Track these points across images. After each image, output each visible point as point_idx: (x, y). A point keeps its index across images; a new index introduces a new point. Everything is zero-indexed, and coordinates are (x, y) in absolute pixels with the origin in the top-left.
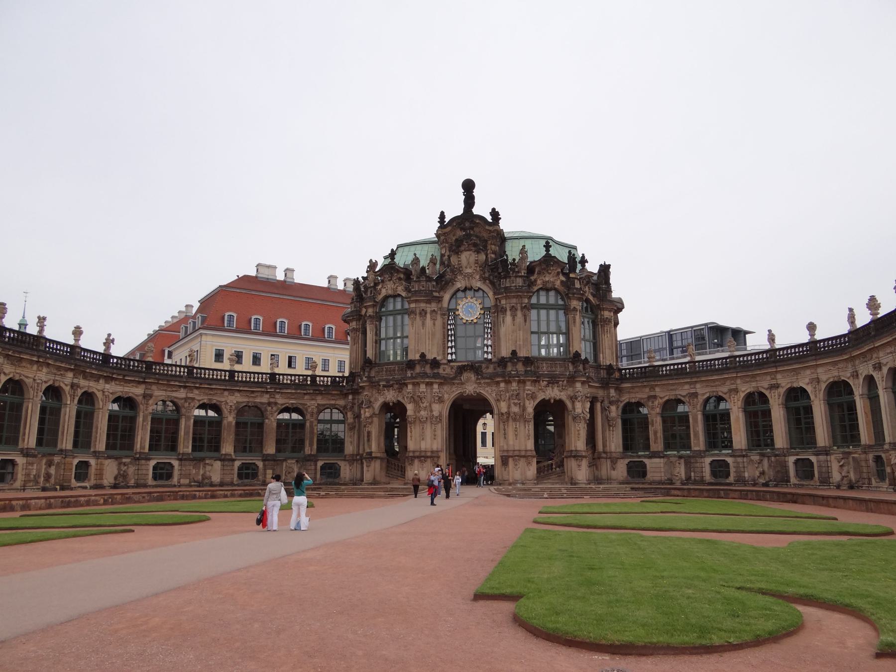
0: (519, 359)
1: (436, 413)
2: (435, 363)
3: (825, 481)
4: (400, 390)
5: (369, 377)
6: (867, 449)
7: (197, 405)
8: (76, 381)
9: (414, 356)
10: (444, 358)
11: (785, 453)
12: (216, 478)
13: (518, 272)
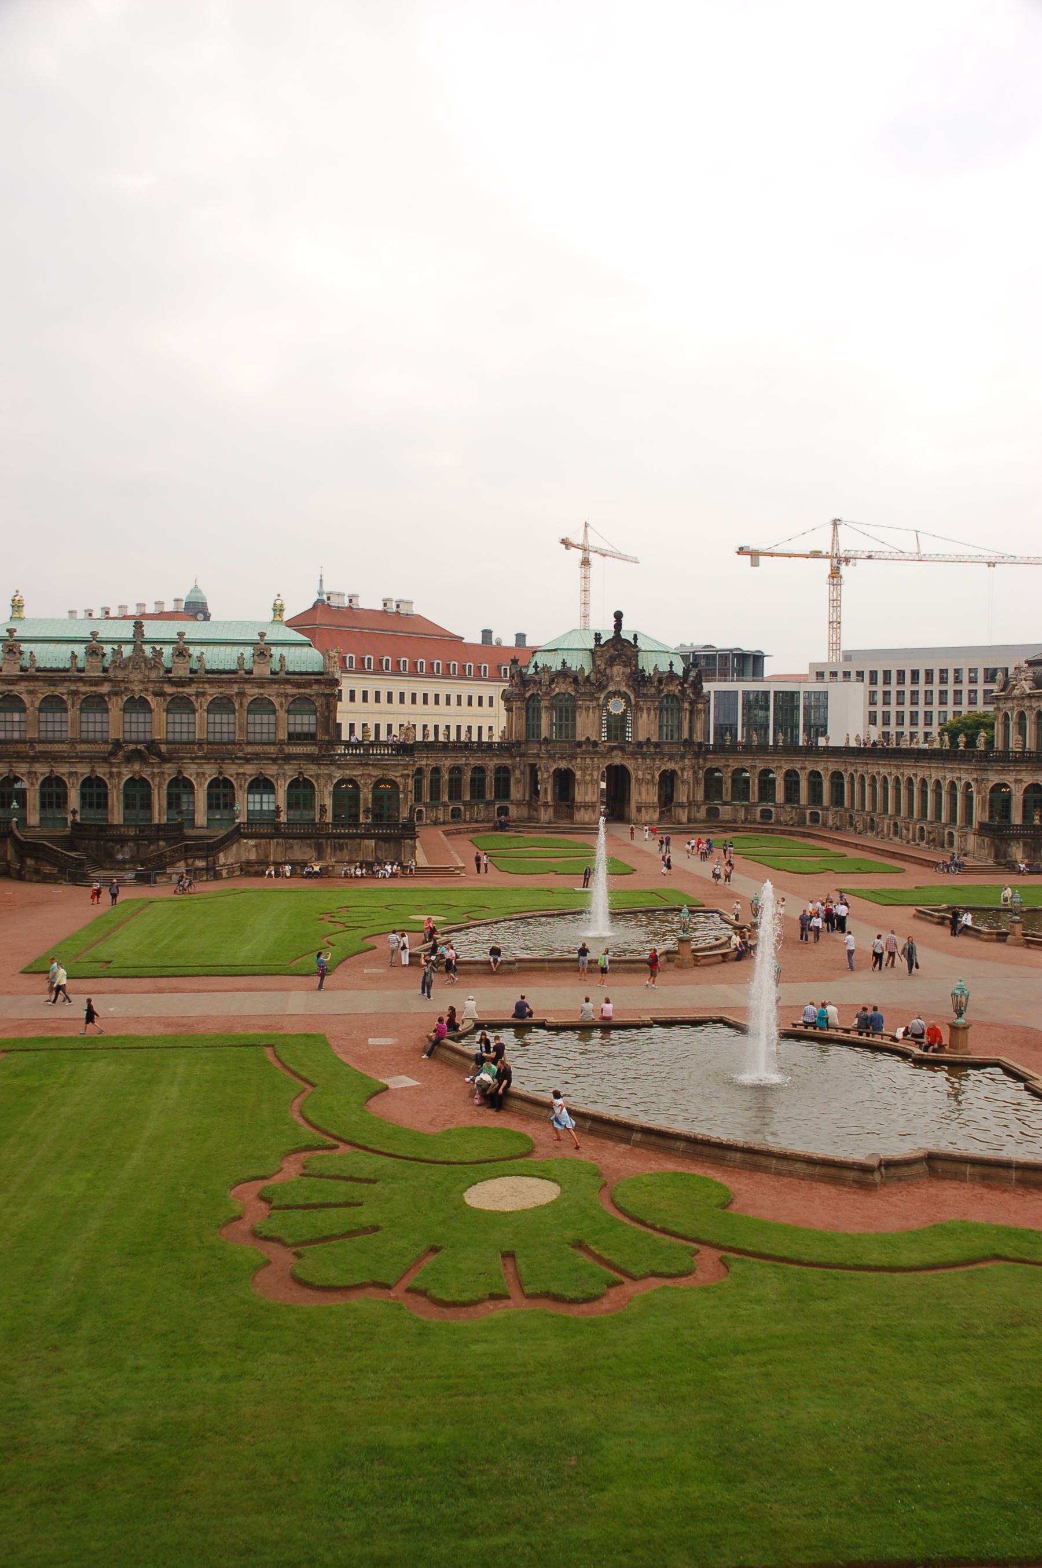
0: (651, 743)
1: (595, 778)
2: (595, 744)
3: (825, 825)
4: (571, 761)
5: (546, 750)
6: (846, 810)
9: (580, 737)
10: (600, 739)
11: (805, 808)
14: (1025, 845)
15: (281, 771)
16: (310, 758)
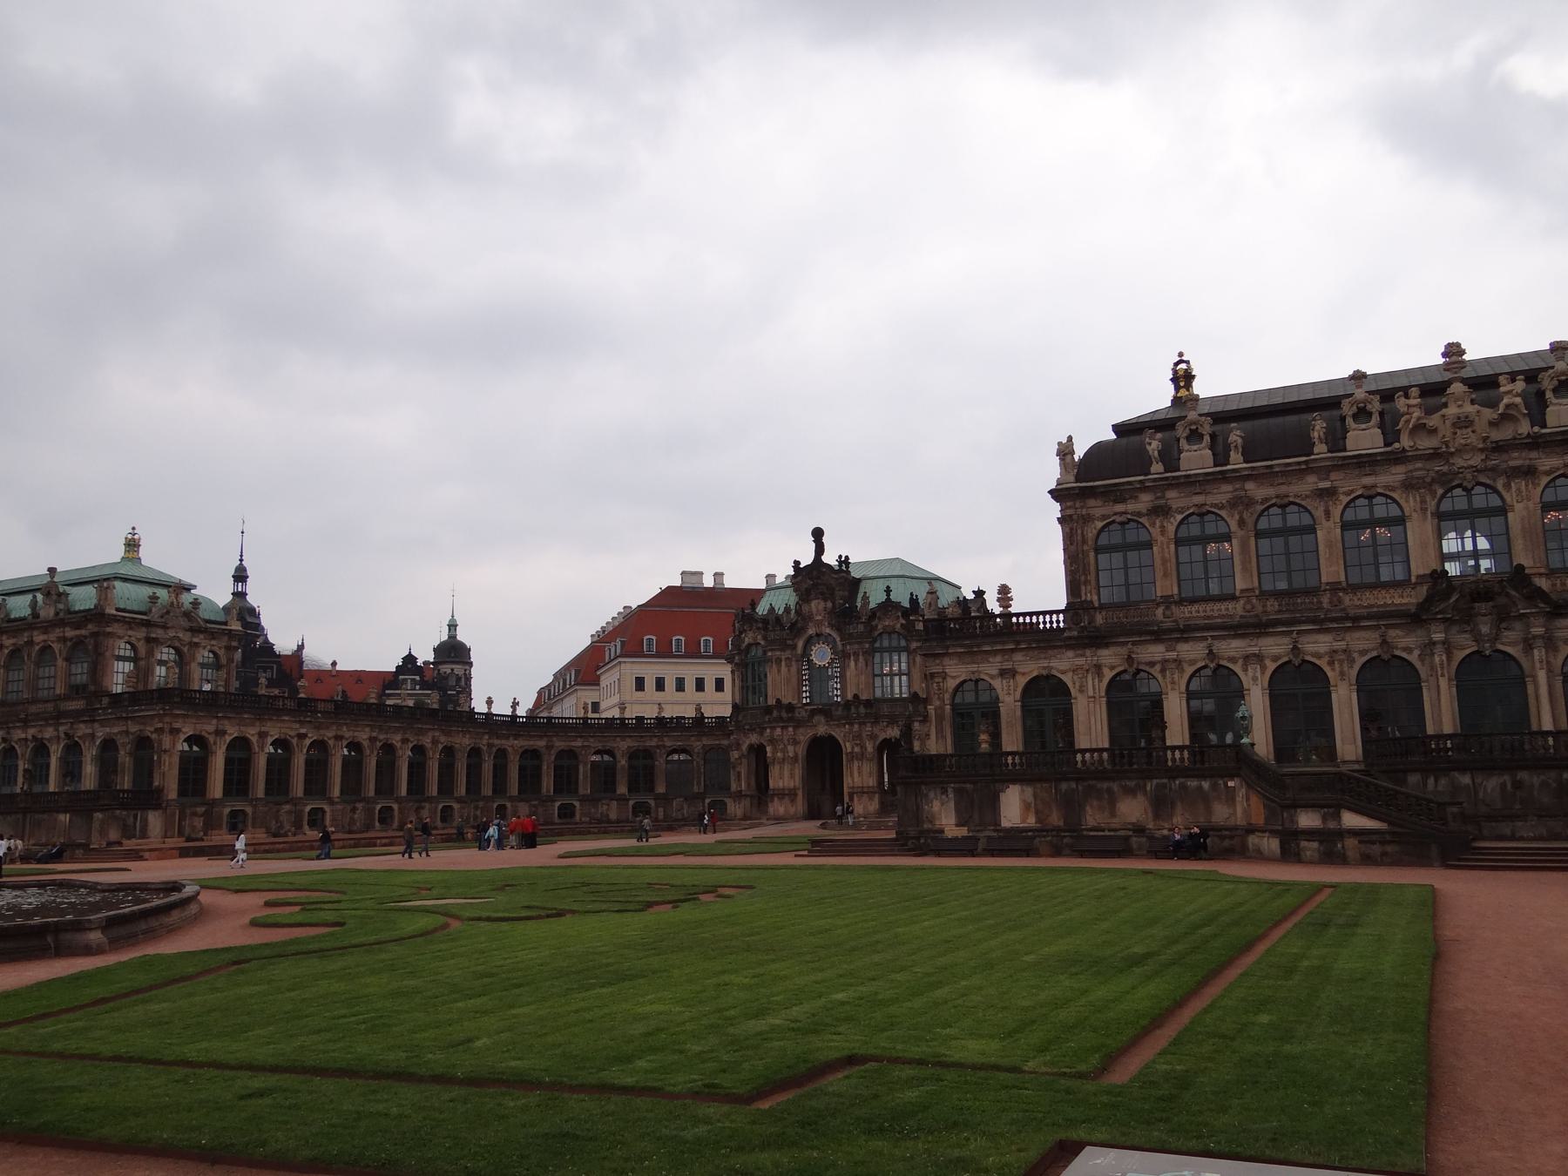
1: (791, 755)
2: (790, 708)
7: (593, 751)
8: (491, 741)
9: (771, 702)
12: (613, 816)
13: (860, 618)
14: (959, 793)
15: (56, 733)
16: (76, 716)
